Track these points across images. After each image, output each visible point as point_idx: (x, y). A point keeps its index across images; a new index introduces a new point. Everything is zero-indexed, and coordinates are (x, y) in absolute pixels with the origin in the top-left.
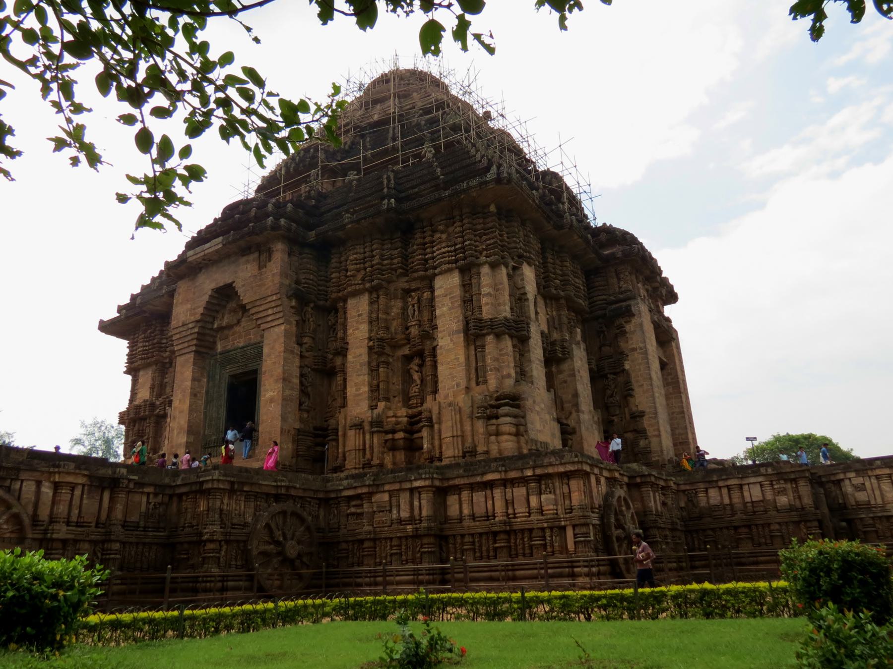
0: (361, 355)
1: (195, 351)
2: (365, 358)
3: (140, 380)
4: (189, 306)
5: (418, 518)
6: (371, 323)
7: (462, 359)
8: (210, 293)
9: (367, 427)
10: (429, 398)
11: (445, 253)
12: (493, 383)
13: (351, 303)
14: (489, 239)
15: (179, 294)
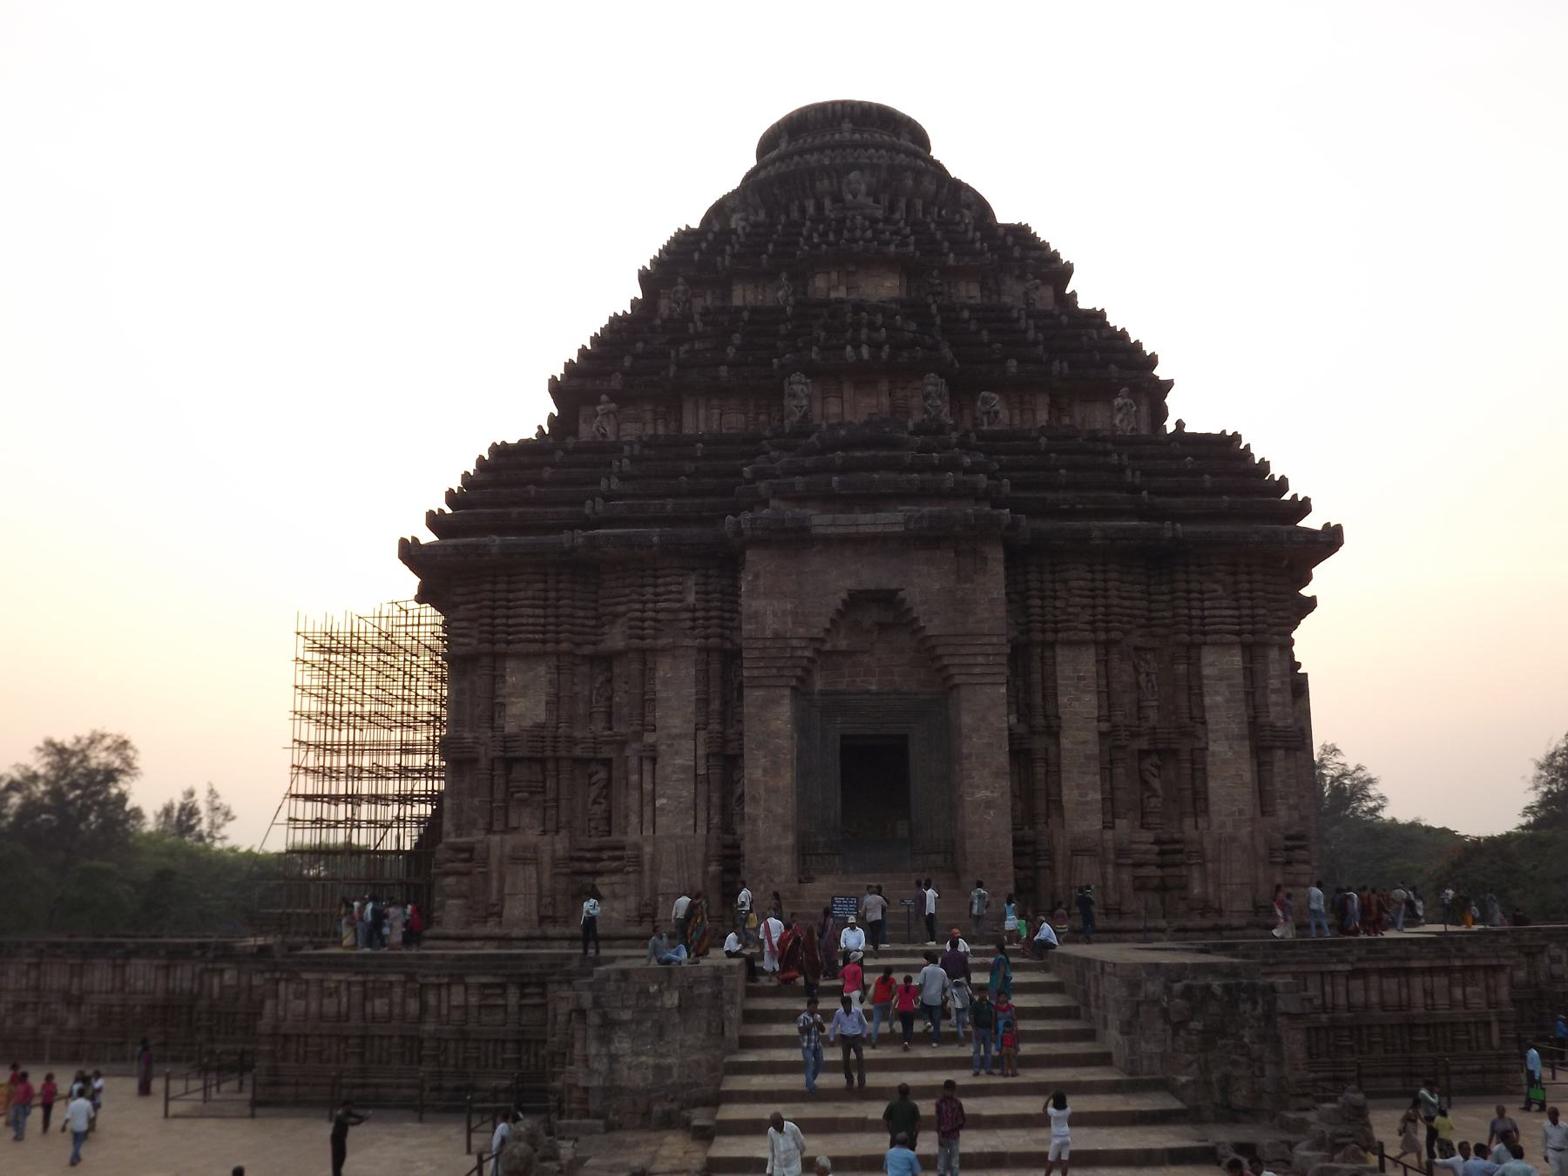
0: (1085, 742)
1: (793, 688)
2: (1094, 749)
3: (511, 680)
4: (789, 606)
5: (1330, 1006)
6: (1099, 693)
7: (1247, 777)
8: (844, 595)
9: (1112, 857)
10: (1188, 822)
11: (1225, 617)
12: (1283, 814)
13: (1062, 654)
14: (1282, 610)
15: (757, 576)
